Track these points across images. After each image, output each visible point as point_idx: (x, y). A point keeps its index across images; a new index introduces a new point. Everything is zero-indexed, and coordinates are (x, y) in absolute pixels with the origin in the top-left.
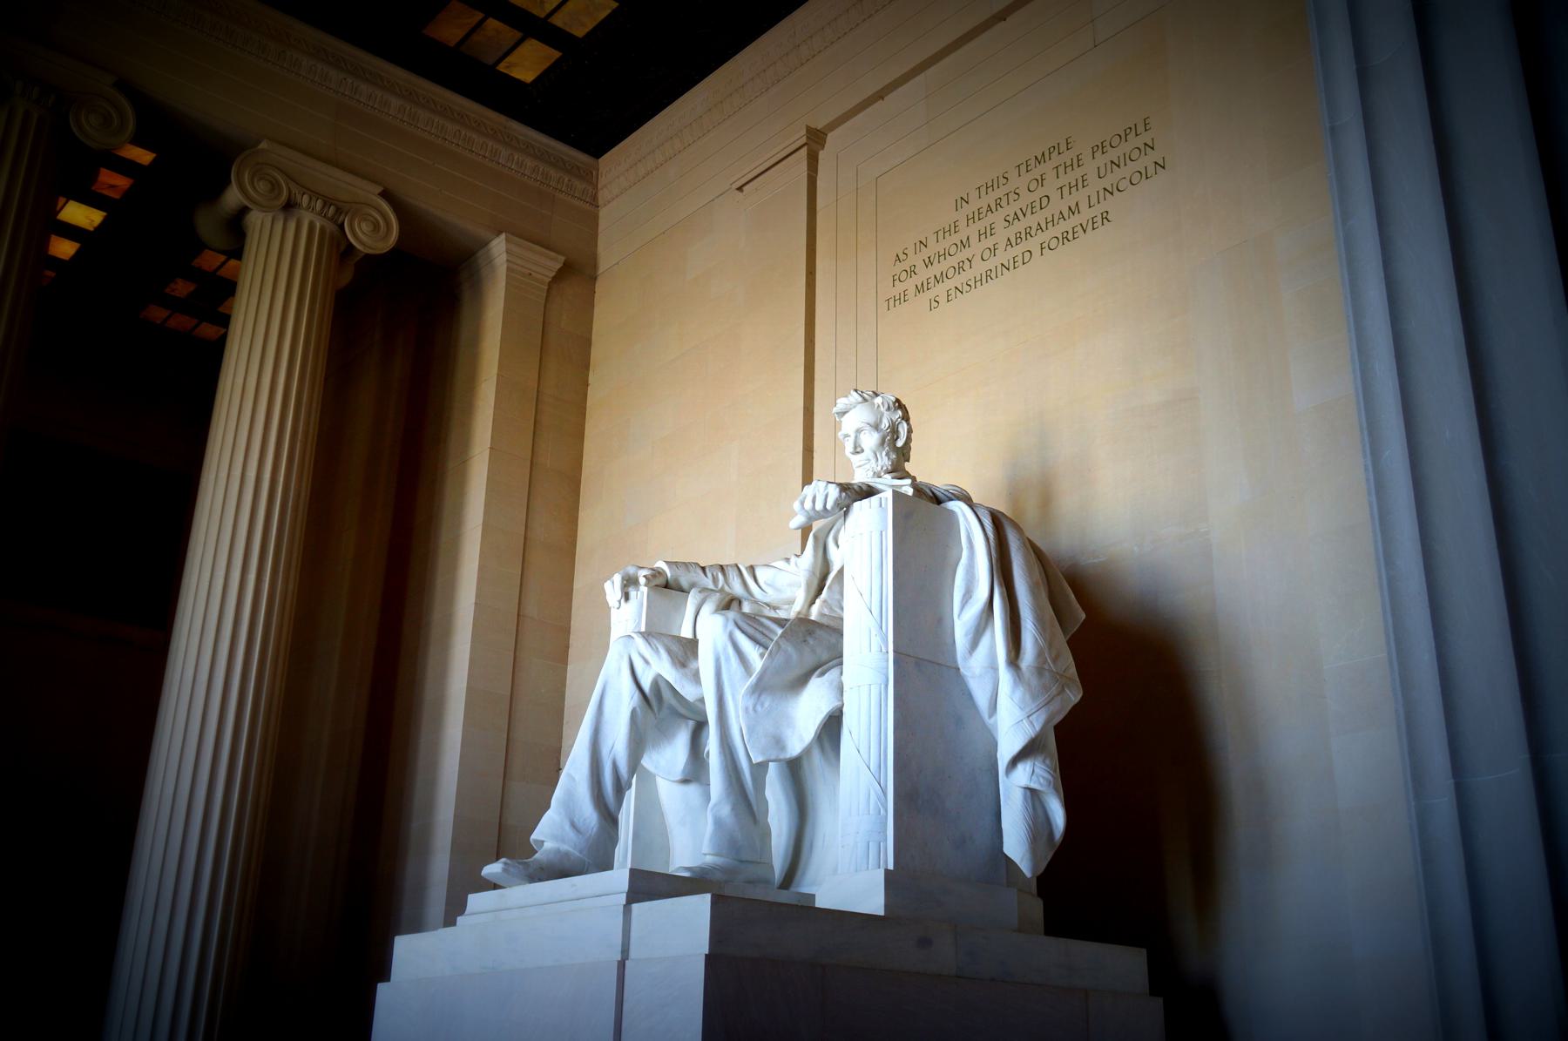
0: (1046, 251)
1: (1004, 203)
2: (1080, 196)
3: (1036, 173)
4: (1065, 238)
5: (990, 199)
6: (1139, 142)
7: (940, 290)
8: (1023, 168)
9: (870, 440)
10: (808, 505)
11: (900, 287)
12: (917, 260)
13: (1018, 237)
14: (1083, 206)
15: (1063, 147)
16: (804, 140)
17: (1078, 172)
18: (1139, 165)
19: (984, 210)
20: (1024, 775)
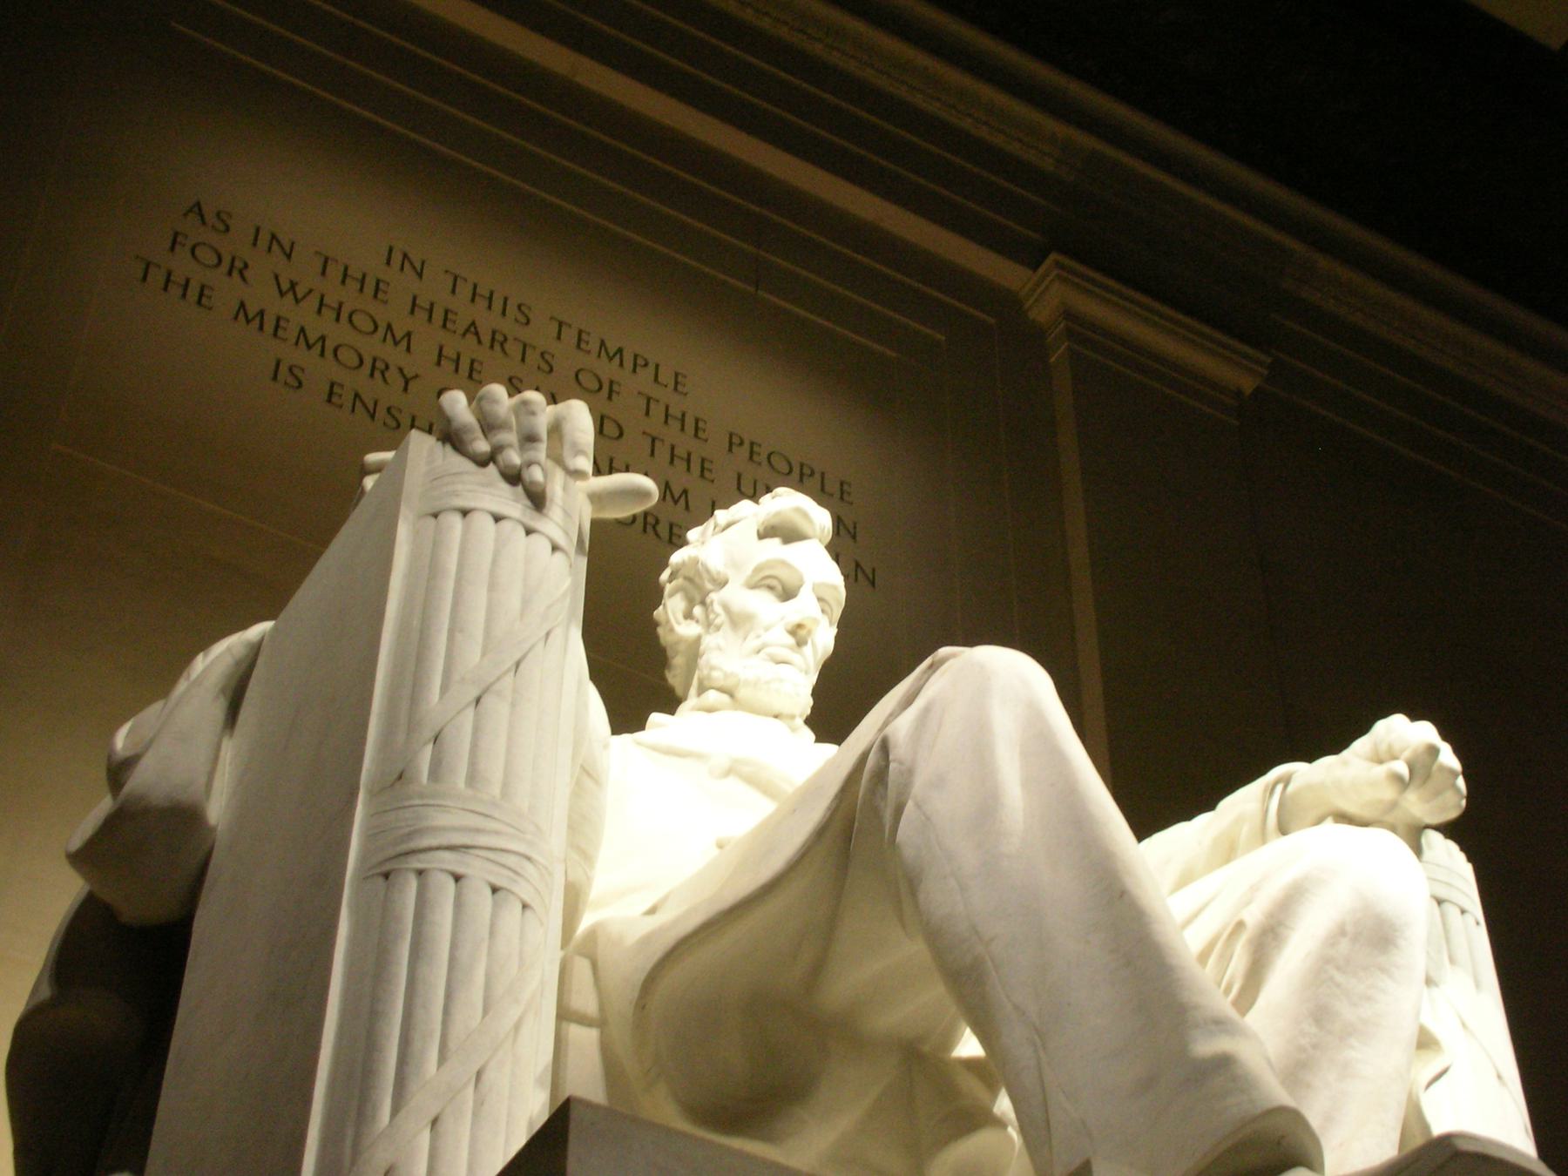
1: (514, 349)
3: (608, 370)
8: (570, 336)
15: (666, 377)
19: (462, 324)
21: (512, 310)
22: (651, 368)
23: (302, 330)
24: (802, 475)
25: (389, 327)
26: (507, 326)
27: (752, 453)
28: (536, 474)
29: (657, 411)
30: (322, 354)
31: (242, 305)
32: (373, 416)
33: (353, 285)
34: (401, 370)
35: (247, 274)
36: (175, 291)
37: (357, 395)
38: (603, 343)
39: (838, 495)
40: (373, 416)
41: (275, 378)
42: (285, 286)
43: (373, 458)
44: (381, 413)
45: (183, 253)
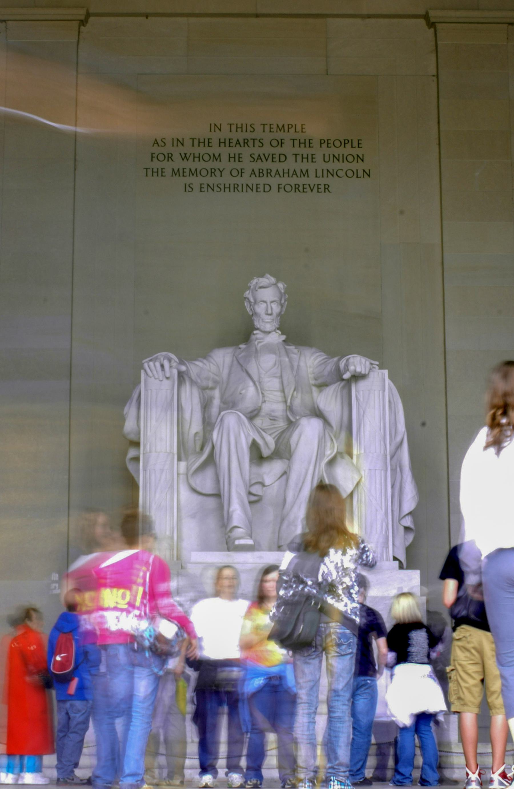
0: (282, 190)
1: (251, 143)
2: (311, 167)
3: (280, 135)
4: (297, 188)
5: (241, 136)
6: (356, 151)
7: (196, 181)
8: (267, 128)
9: (276, 309)
10: (358, 370)
11: (156, 165)
12: (176, 151)
13: (261, 171)
14: (312, 173)
15: (299, 128)
16: (82, 18)
17: (310, 151)
18: (354, 166)
19: (234, 141)
20: (408, 522)
21: (249, 128)
22: (294, 126)
23: (190, 170)
24: (345, 144)
25: (214, 155)
26: (249, 135)
27: (328, 143)
28: (161, 378)
29: (297, 143)
30: (197, 176)
31: (173, 170)
32: (213, 190)
33: (202, 145)
34: (219, 169)
35: (172, 158)
36: (155, 174)
37: (208, 185)
38: (278, 126)
39: (357, 146)
40: (213, 190)
41: (186, 191)
42: (183, 156)
43: (144, 361)
44: (216, 188)
45: (155, 159)
